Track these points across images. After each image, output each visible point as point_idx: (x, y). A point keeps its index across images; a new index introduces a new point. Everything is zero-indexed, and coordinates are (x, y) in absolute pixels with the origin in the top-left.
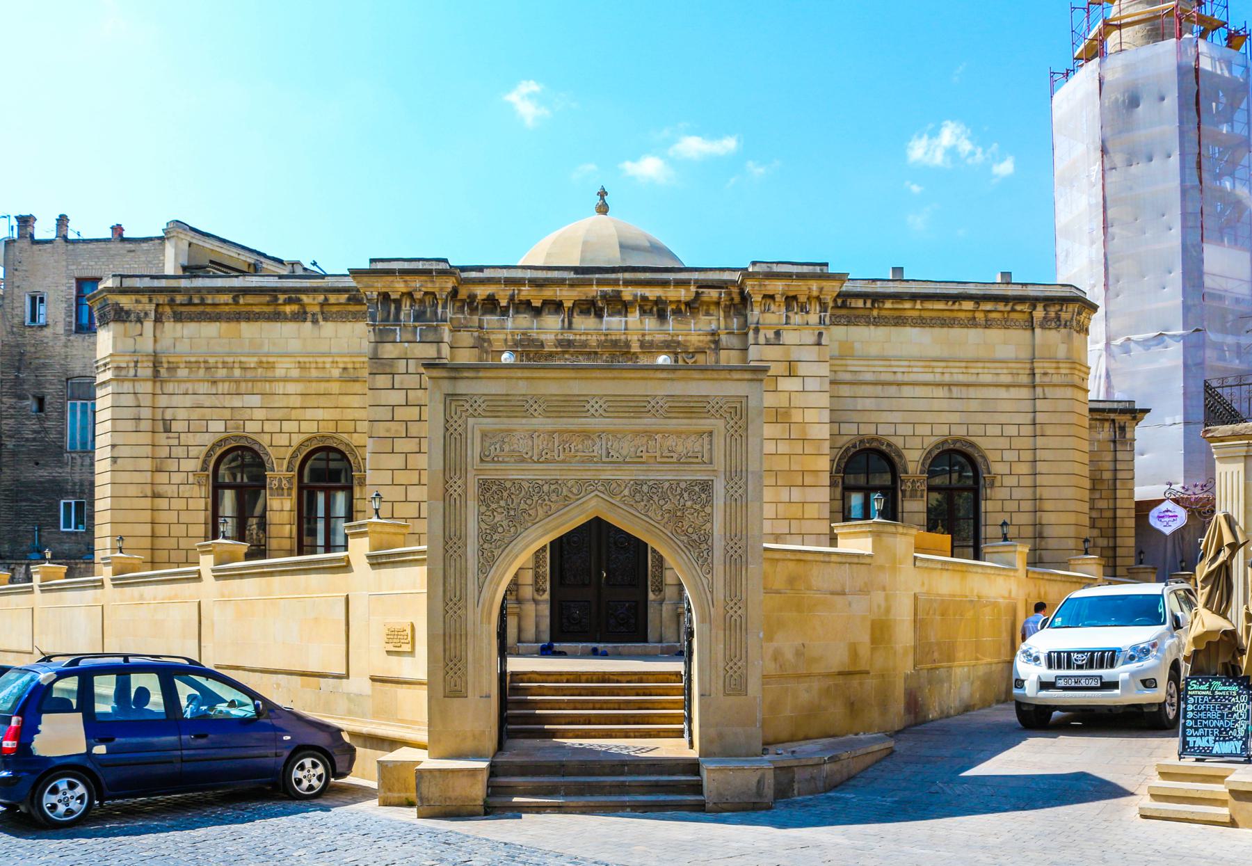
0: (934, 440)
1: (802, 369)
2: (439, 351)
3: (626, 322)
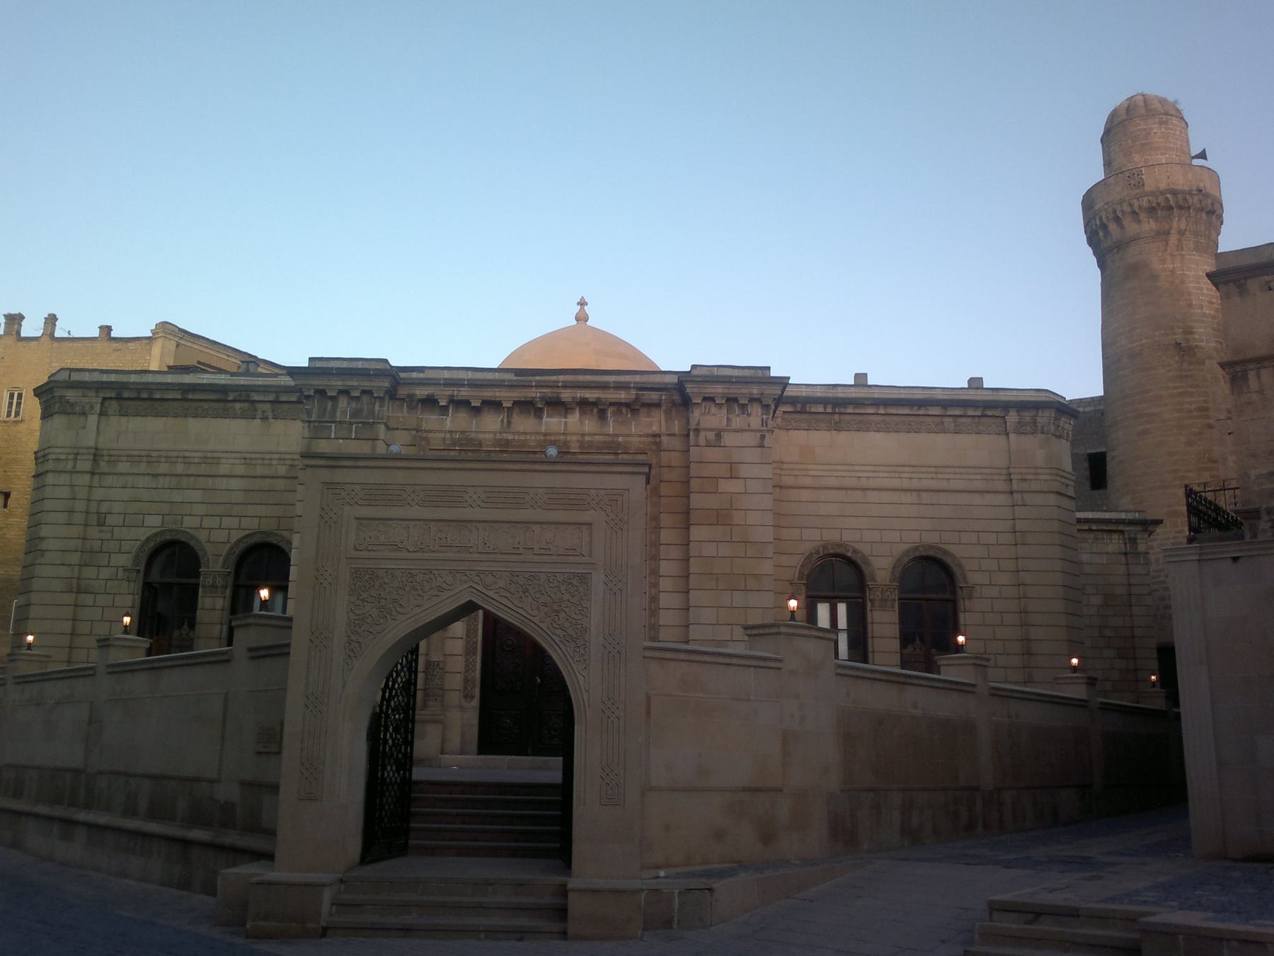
0: (905, 547)
1: (744, 471)
2: (374, 447)
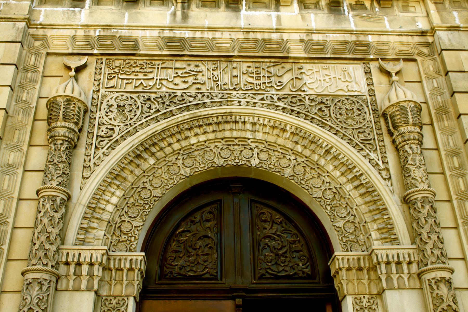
3: (278, 18)
